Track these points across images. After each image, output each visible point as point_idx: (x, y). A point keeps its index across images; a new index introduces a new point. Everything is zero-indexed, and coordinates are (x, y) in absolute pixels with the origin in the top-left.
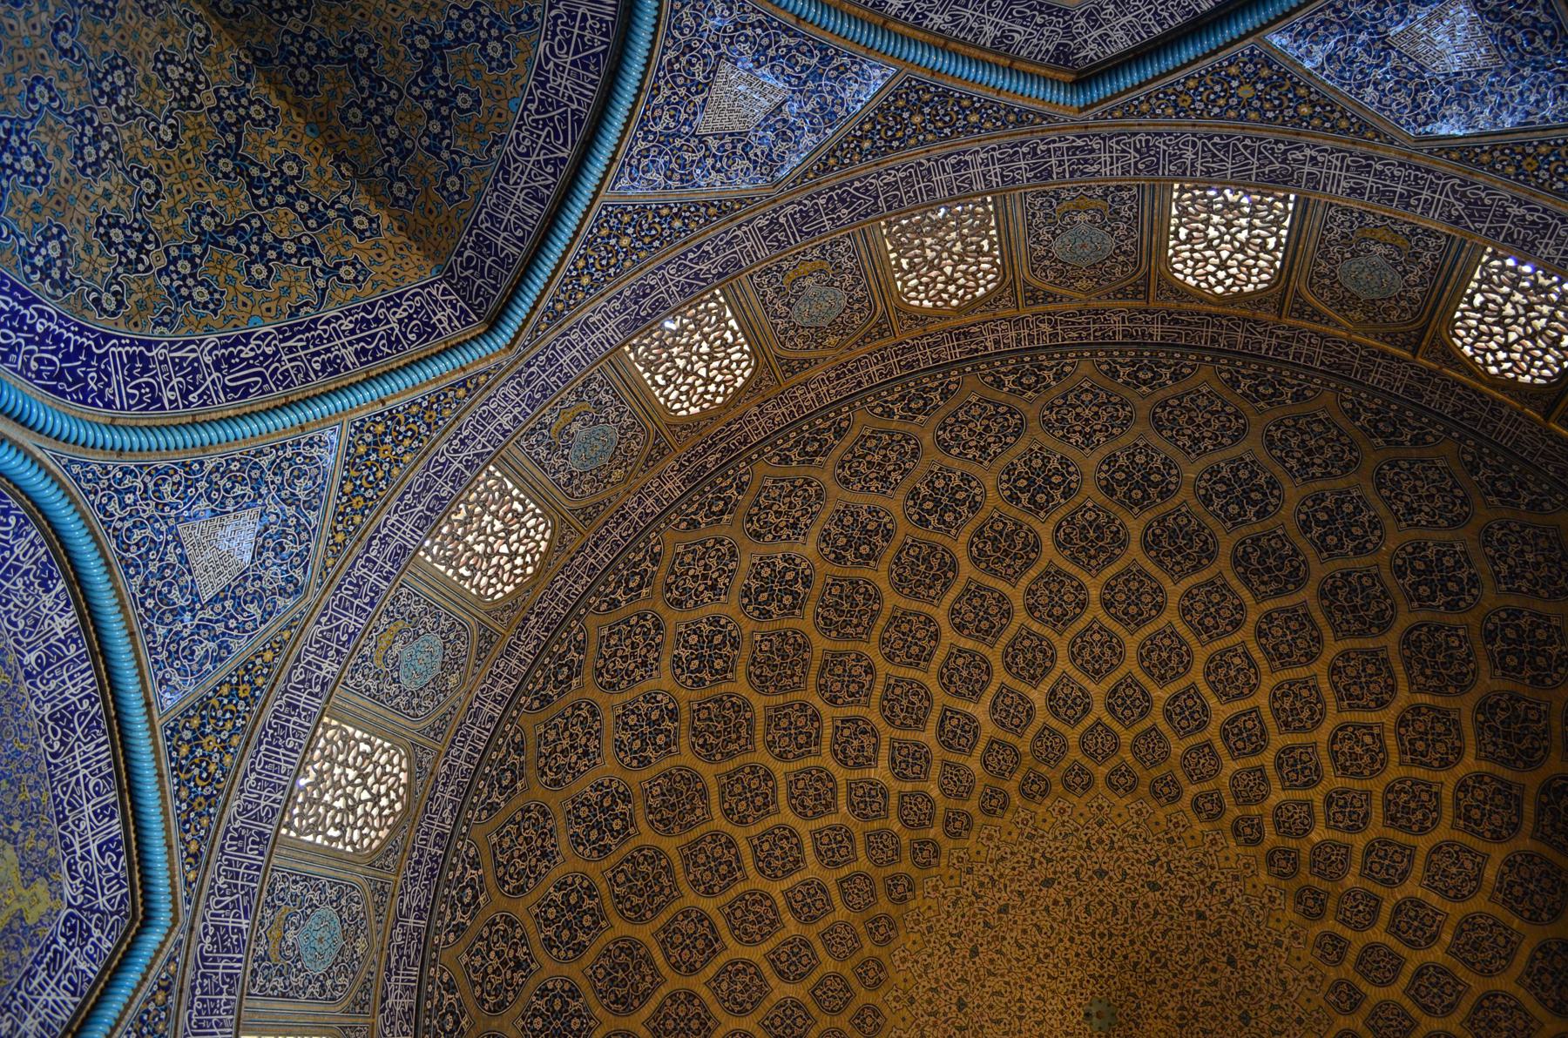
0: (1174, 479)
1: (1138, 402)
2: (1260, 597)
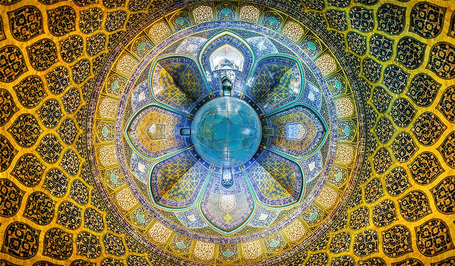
0: (400, 101)
1: (379, 117)
2: (424, 46)
